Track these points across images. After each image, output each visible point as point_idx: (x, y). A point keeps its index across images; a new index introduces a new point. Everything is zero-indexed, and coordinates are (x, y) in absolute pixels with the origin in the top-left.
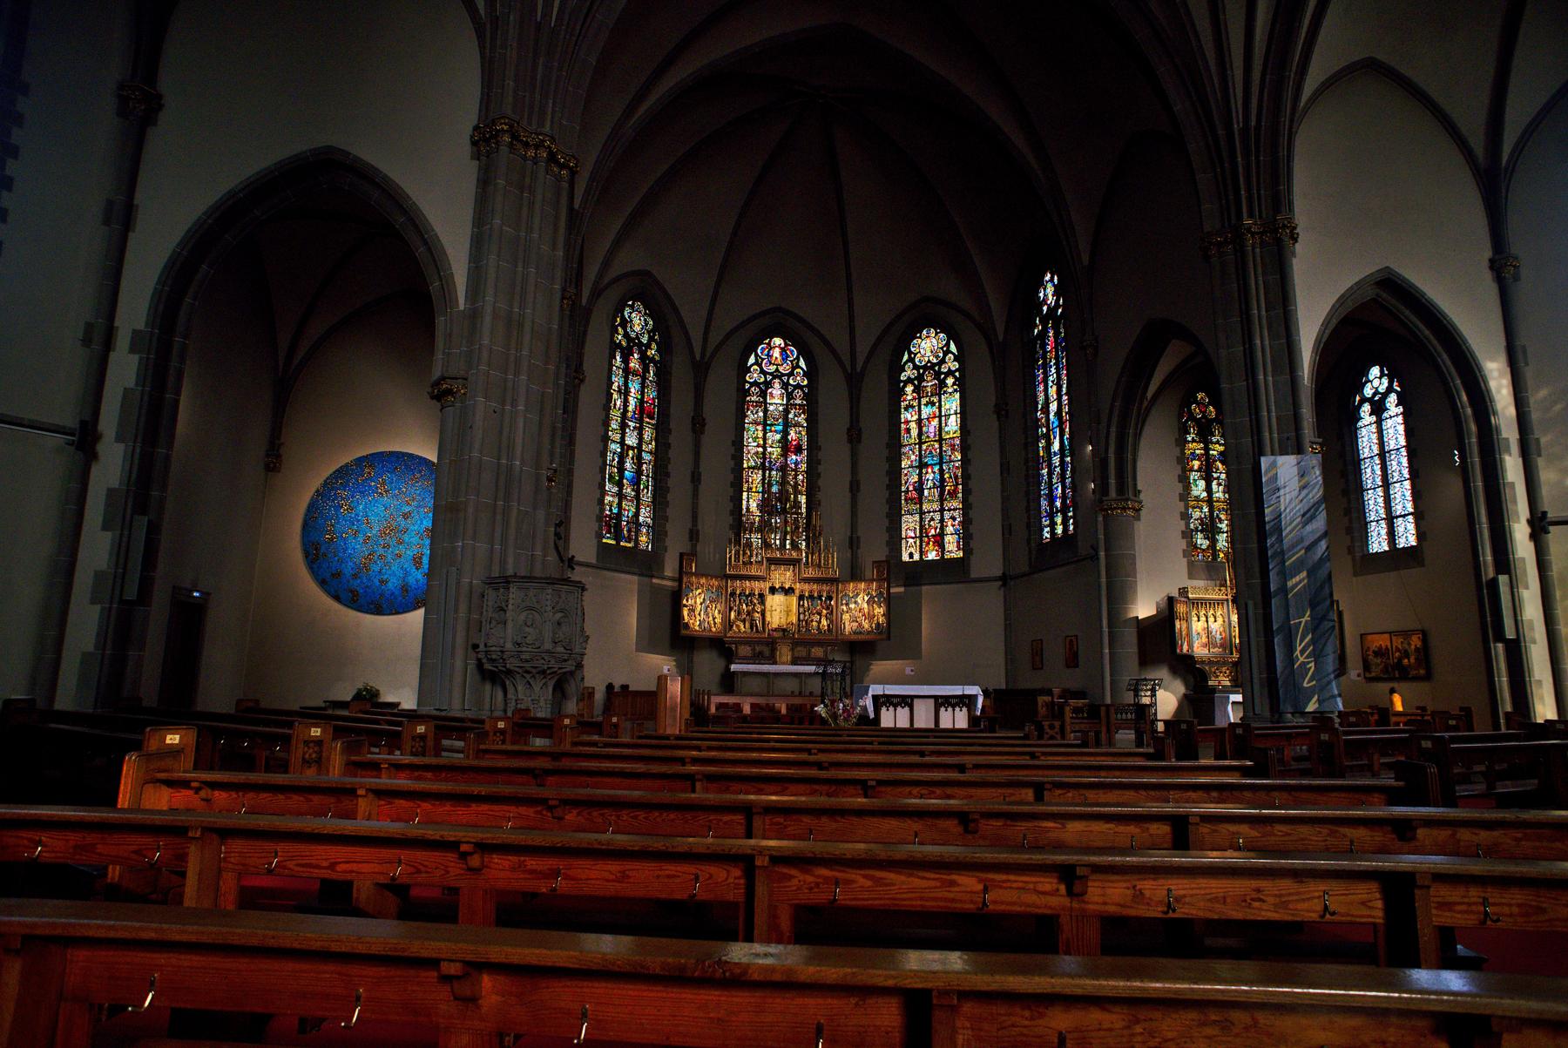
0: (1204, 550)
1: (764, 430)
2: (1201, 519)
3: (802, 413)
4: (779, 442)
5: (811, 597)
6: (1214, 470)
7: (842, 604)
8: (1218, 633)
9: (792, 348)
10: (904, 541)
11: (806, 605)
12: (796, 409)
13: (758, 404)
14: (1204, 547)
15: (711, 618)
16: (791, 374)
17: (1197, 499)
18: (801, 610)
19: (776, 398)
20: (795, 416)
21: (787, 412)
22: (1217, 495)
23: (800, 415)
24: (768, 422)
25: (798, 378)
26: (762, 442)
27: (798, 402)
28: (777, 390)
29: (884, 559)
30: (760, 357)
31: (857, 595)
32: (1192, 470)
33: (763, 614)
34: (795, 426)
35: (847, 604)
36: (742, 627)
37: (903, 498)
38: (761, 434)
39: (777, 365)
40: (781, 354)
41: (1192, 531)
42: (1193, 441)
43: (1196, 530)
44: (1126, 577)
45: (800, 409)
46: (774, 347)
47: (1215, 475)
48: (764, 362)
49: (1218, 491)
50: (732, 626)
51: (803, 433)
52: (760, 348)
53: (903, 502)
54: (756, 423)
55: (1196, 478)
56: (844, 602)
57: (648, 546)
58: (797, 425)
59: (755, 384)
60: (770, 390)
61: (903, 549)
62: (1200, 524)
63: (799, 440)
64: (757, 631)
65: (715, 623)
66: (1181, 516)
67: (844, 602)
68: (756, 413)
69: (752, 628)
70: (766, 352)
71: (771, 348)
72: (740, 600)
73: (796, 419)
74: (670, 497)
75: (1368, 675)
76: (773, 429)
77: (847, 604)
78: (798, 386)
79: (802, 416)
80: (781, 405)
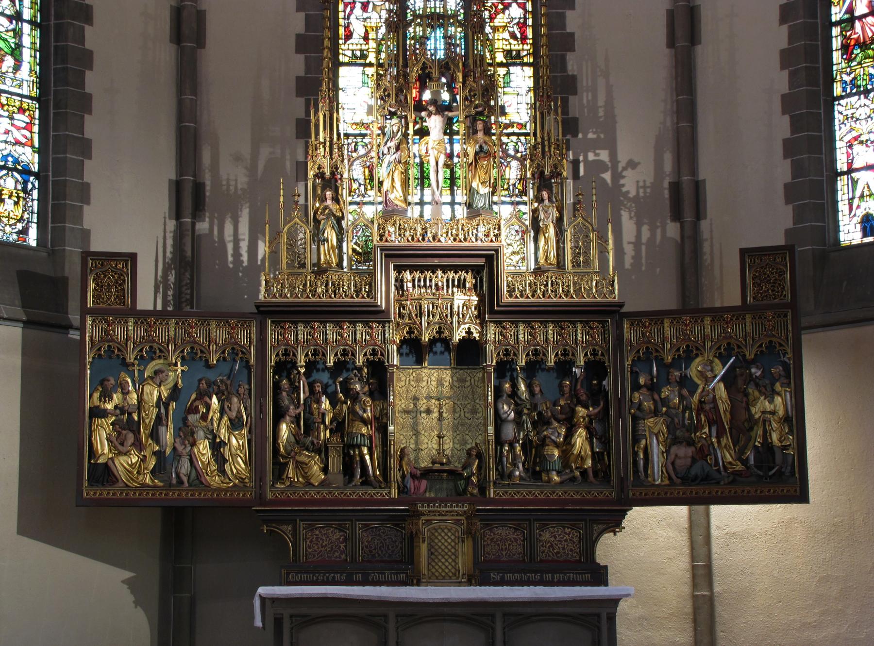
5: (534, 367)
10: (842, 183)
15: (204, 449)
29: (780, 241)
31: (689, 357)
33: (381, 424)
35: (653, 388)
36: (316, 468)
37: (836, 43)
50: (280, 469)
53: (836, 56)
57: (24, 231)
61: (843, 207)
64: (366, 481)
65: (220, 459)
69: (348, 469)
72: (311, 386)
74: (92, 82)
77: (653, 388)
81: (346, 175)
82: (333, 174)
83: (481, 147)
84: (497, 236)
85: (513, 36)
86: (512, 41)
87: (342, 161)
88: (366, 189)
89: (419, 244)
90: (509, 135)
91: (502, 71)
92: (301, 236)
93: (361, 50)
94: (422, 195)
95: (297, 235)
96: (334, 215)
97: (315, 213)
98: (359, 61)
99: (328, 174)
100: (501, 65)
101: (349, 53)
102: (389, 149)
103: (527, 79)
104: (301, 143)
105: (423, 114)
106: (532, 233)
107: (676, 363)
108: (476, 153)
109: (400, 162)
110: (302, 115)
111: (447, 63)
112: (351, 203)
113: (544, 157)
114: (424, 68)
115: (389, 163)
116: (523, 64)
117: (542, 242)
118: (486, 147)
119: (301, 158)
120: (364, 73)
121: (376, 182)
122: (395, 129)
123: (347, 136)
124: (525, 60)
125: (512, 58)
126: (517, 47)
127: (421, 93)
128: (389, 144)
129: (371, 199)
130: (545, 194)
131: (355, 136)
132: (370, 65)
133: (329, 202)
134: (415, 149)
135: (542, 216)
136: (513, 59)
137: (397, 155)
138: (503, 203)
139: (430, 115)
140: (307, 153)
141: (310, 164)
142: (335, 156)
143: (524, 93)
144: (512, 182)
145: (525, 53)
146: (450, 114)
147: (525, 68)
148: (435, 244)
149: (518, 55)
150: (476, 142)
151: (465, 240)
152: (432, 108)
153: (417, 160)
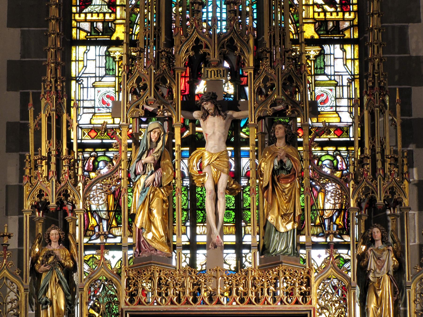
81: (80, 205)
82: (60, 203)
83: (281, 162)
84: (305, 295)
86: (326, 7)
87: (75, 184)
88: (110, 226)
89: (189, 307)
90: (322, 145)
91: (313, 51)
92: (12, 296)
93: (104, 22)
94: (194, 234)
95: (6, 295)
96: (62, 265)
97: (34, 262)
98: (101, 38)
99: (53, 204)
100: (311, 42)
101: (86, 26)
102: (145, 166)
103: (349, 63)
104: (15, 157)
105: (196, 114)
106: (358, 291)
108: (274, 172)
109: (160, 186)
110: (16, 118)
111: (231, 40)
112: (88, 247)
113: (374, 178)
114: (197, 46)
115: (145, 187)
116: (343, 42)
117: (372, 305)
118: (288, 163)
119: (13, 181)
120: (108, 55)
121: (125, 215)
122: (154, 136)
123: (82, 146)
124: (347, 35)
125: (327, 32)
126: (334, 16)
127: (192, 85)
128: (144, 159)
129: (118, 240)
130: (377, 232)
131: (94, 146)
132: (118, 43)
133: (54, 246)
134: (184, 165)
135: (372, 264)
137: (155, 176)
138: (316, 246)
139: (205, 116)
140: (22, 172)
141: (26, 190)
142: (65, 177)
143: (345, 82)
144: (327, 214)
145: (347, 24)
146: (236, 115)
147: (348, 47)
148: (213, 307)
149: (337, 29)
150: (274, 155)
151: (257, 300)
152: (208, 106)
153: (187, 182)
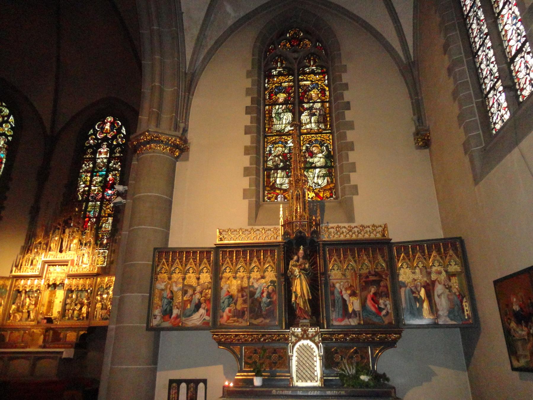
0: (285, 191)
1: (92, 177)
2: (284, 155)
3: (119, 162)
4: (100, 182)
6: (306, 100)
7: (97, 295)
8: (265, 294)
9: (118, 122)
11: (74, 296)
12: (115, 160)
13: (90, 159)
14: (285, 186)
16: (114, 138)
17: (280, 133)
18: (68, 301)
19: (103, 155)
20: (114, 164)
21: (109, 162)
22: (308, 126)
23: (117, 163)
24: (96, 170)
25: (120, 140)
26: (88, 183)
27: (118, 155)
28: (104, 149)
30: (96, 130)
32: (275, 103)
34: (112, 171)
38: (89, 178)
39: (106, 133)
40: (110, 126)
41: (270, 169)
42: (280, 74)
43: (276, 168)
44: (139, 224)
45: (117, 160)
46: (107, 123)
47: (306, 106)
48: (99, 132)
49: (311, 122)
51: (118, 175)
52: (98, 124)
54: (87, 171)
55: (280, 111)
56: (99, 293)
58: (116, 169)
59: (91, 146)
60: (99, 150)
62: (281, 161)
63: (115, 179)
66: (245, 150)
67: (99, 293)
68: (89, 164)
70: (101, 126)
71: (105, 123)
73: (114, 166)
75: (516, 364)
76: (98, 174)
78: (118, 145)
79: (119, 163)
80: (105, 158)
85: (110, 210)
91: (106, 218)
107: (106, 289)
136: (109, 215)
